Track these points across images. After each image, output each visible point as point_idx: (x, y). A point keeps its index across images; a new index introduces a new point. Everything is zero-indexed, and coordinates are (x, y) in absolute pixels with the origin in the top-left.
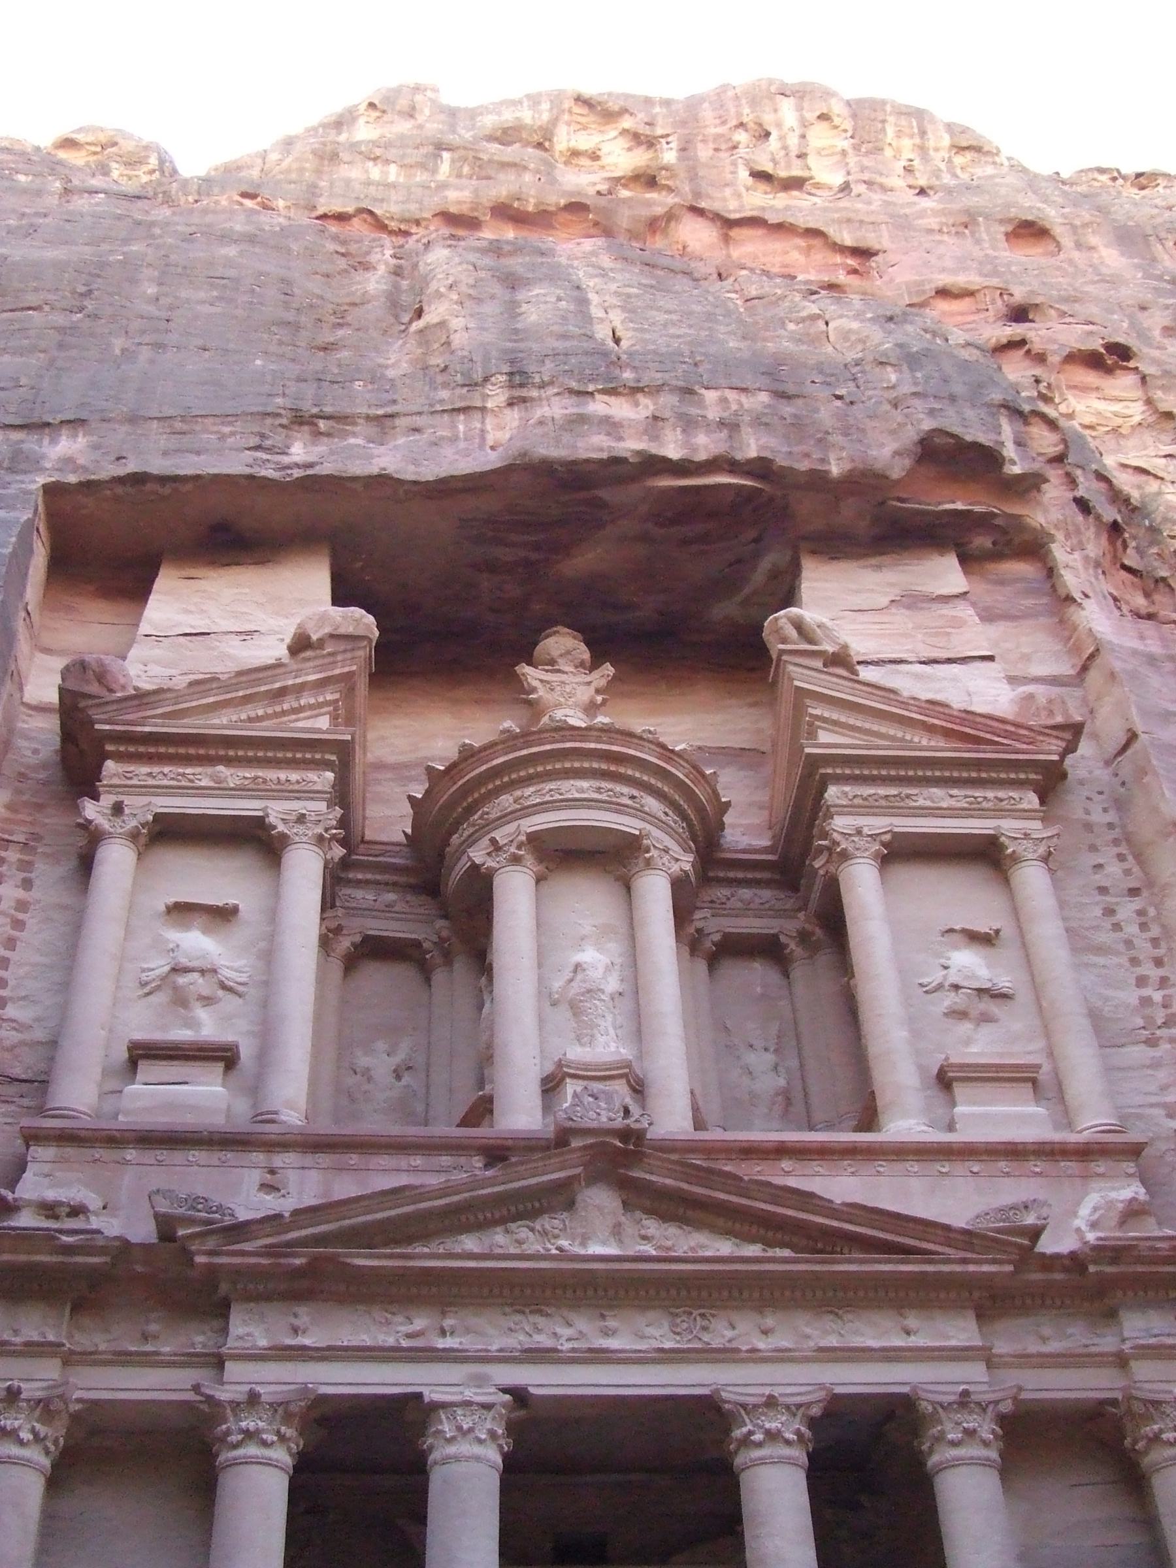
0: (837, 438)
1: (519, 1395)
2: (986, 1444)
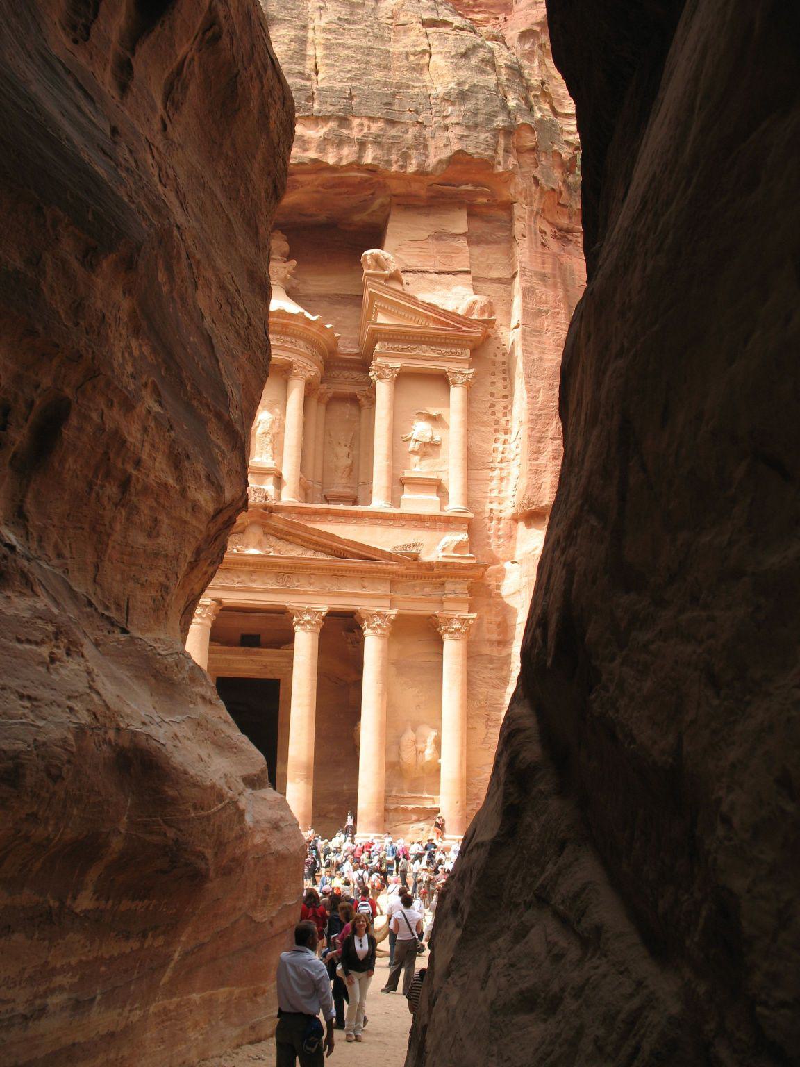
1: (219, 602)
2: (384, 629)
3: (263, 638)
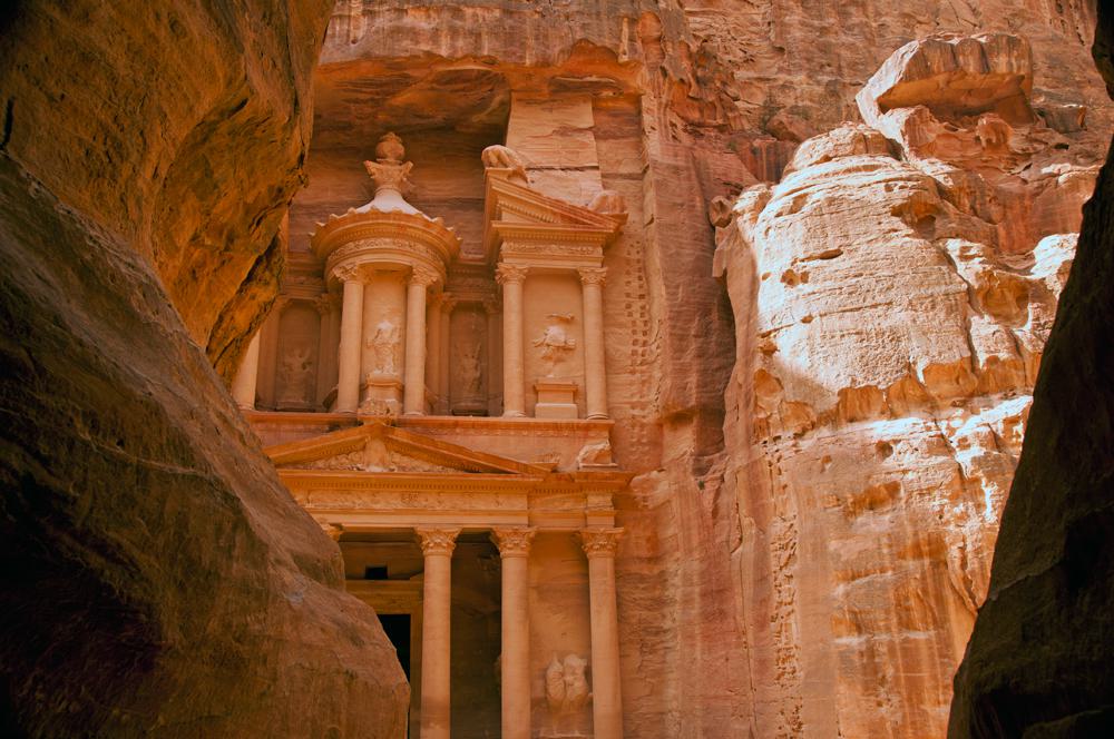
0: (531, 42)
1: (338, 526)
2: (522, 549)
3: (390, 571)
